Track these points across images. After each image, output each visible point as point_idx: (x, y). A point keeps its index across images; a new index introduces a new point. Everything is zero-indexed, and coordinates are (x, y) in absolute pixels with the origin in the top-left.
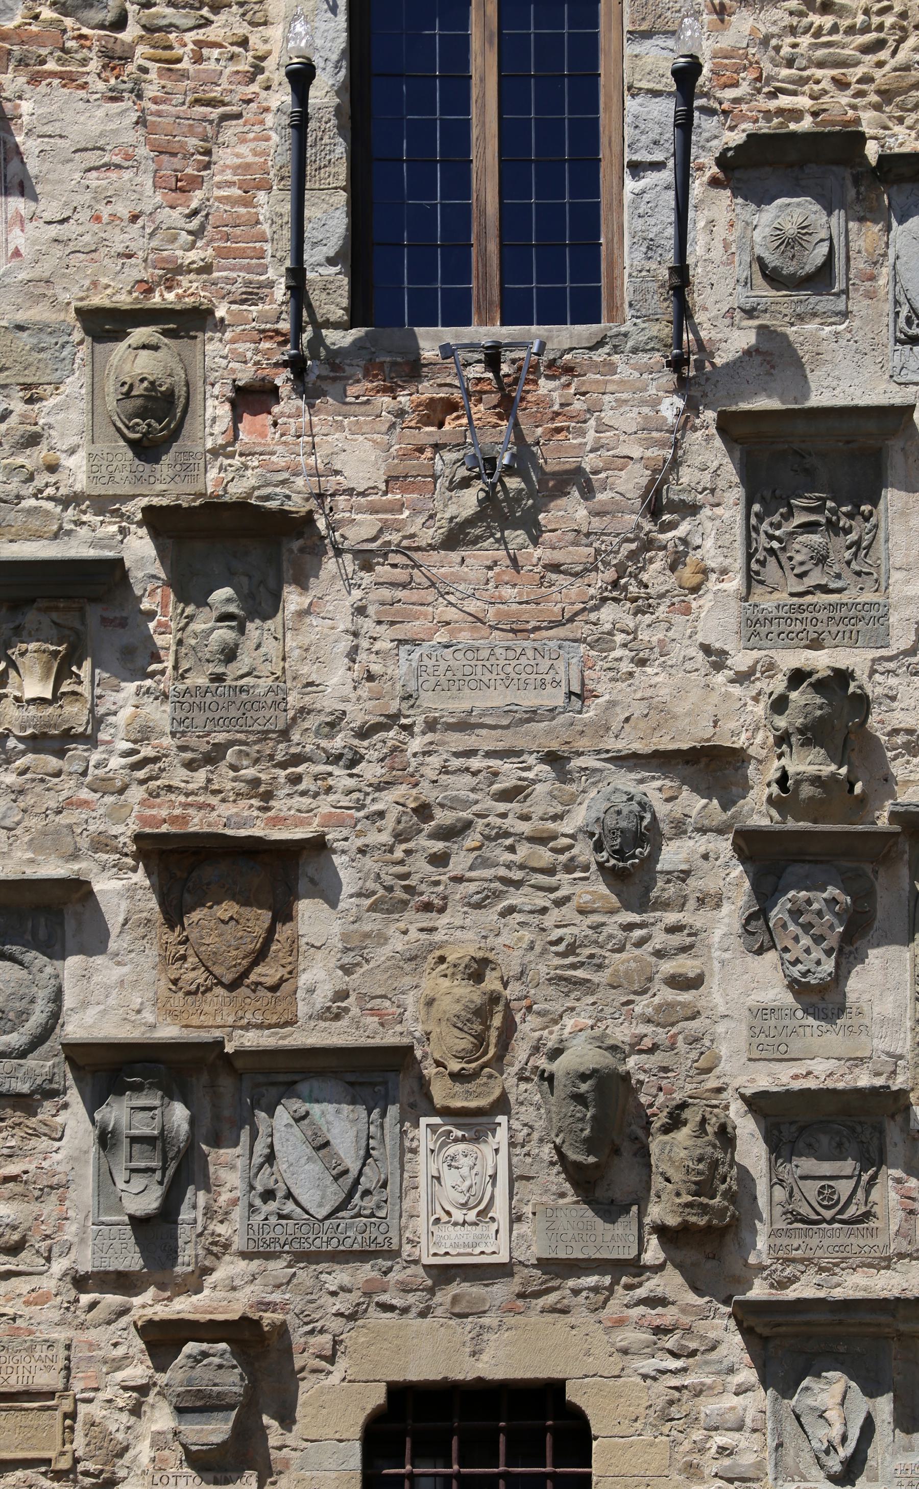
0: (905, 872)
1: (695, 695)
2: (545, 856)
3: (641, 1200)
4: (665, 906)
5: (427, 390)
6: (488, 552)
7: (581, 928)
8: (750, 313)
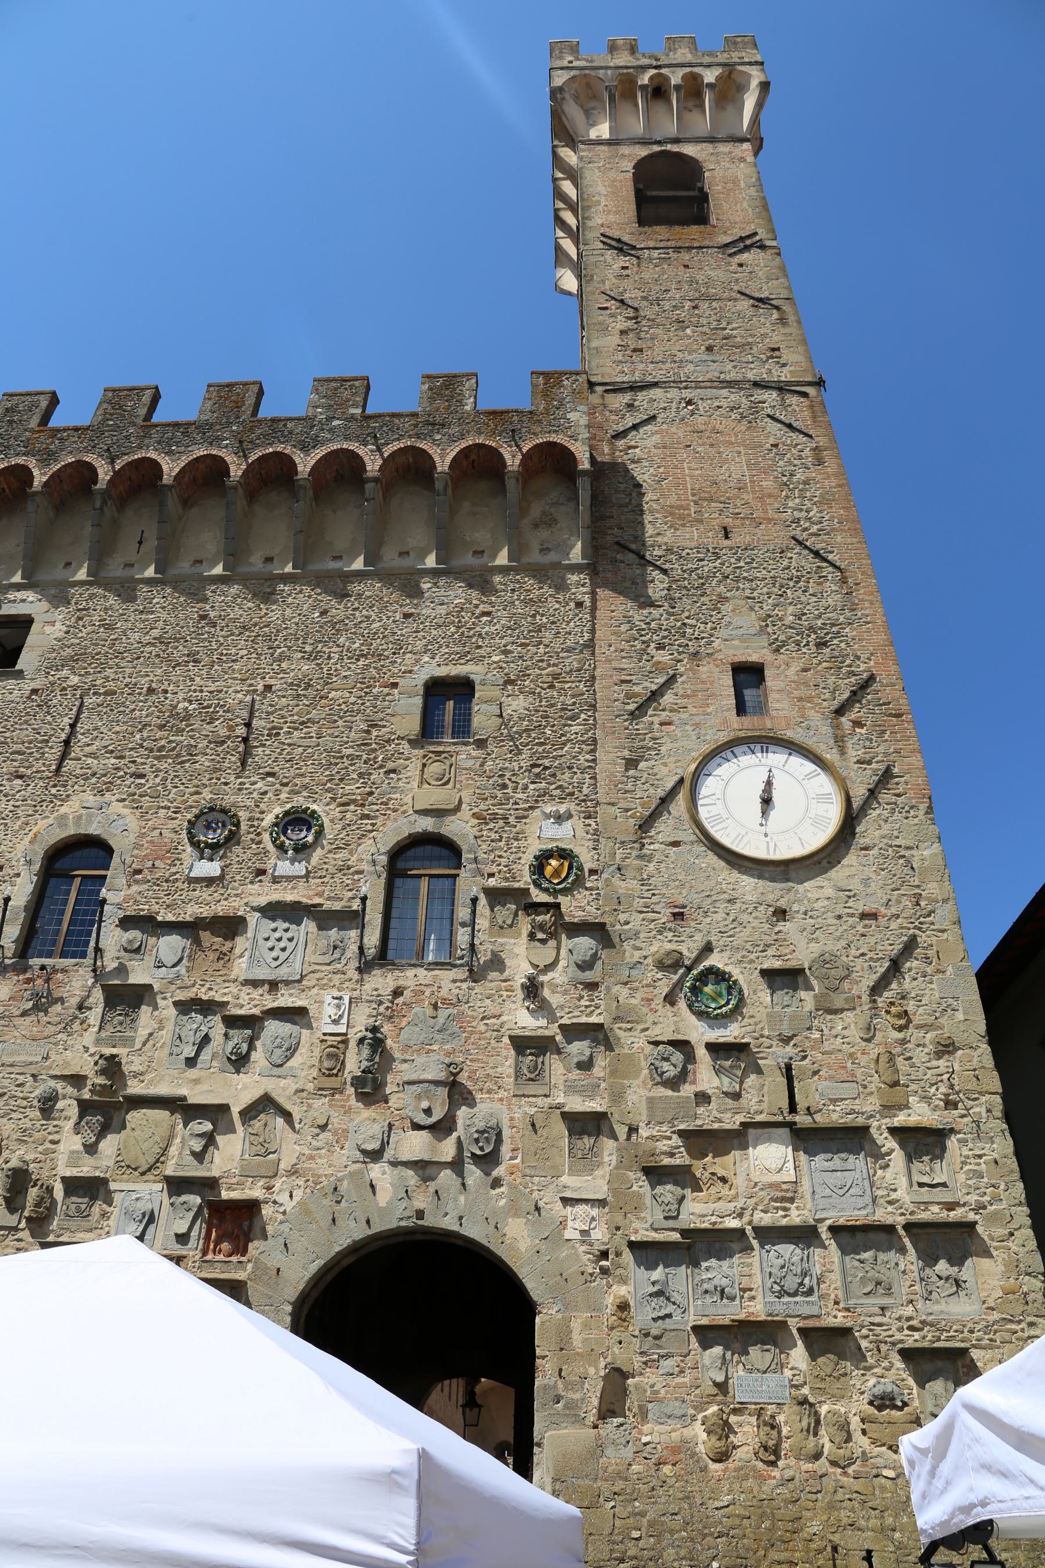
0: (124, 1112)
1: (78, 1059)
2: (25, 1103)
3: (23, 1208)
4: (55, 1119)
5: (28, 975)
6: (33, 1018)
7: (29, 1125)
8: (118, 958)
